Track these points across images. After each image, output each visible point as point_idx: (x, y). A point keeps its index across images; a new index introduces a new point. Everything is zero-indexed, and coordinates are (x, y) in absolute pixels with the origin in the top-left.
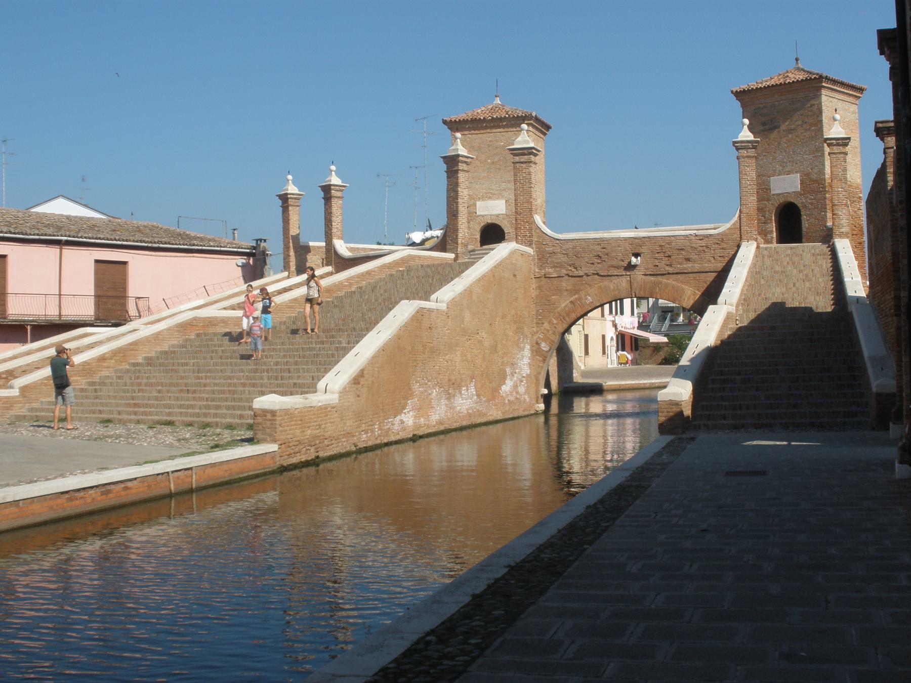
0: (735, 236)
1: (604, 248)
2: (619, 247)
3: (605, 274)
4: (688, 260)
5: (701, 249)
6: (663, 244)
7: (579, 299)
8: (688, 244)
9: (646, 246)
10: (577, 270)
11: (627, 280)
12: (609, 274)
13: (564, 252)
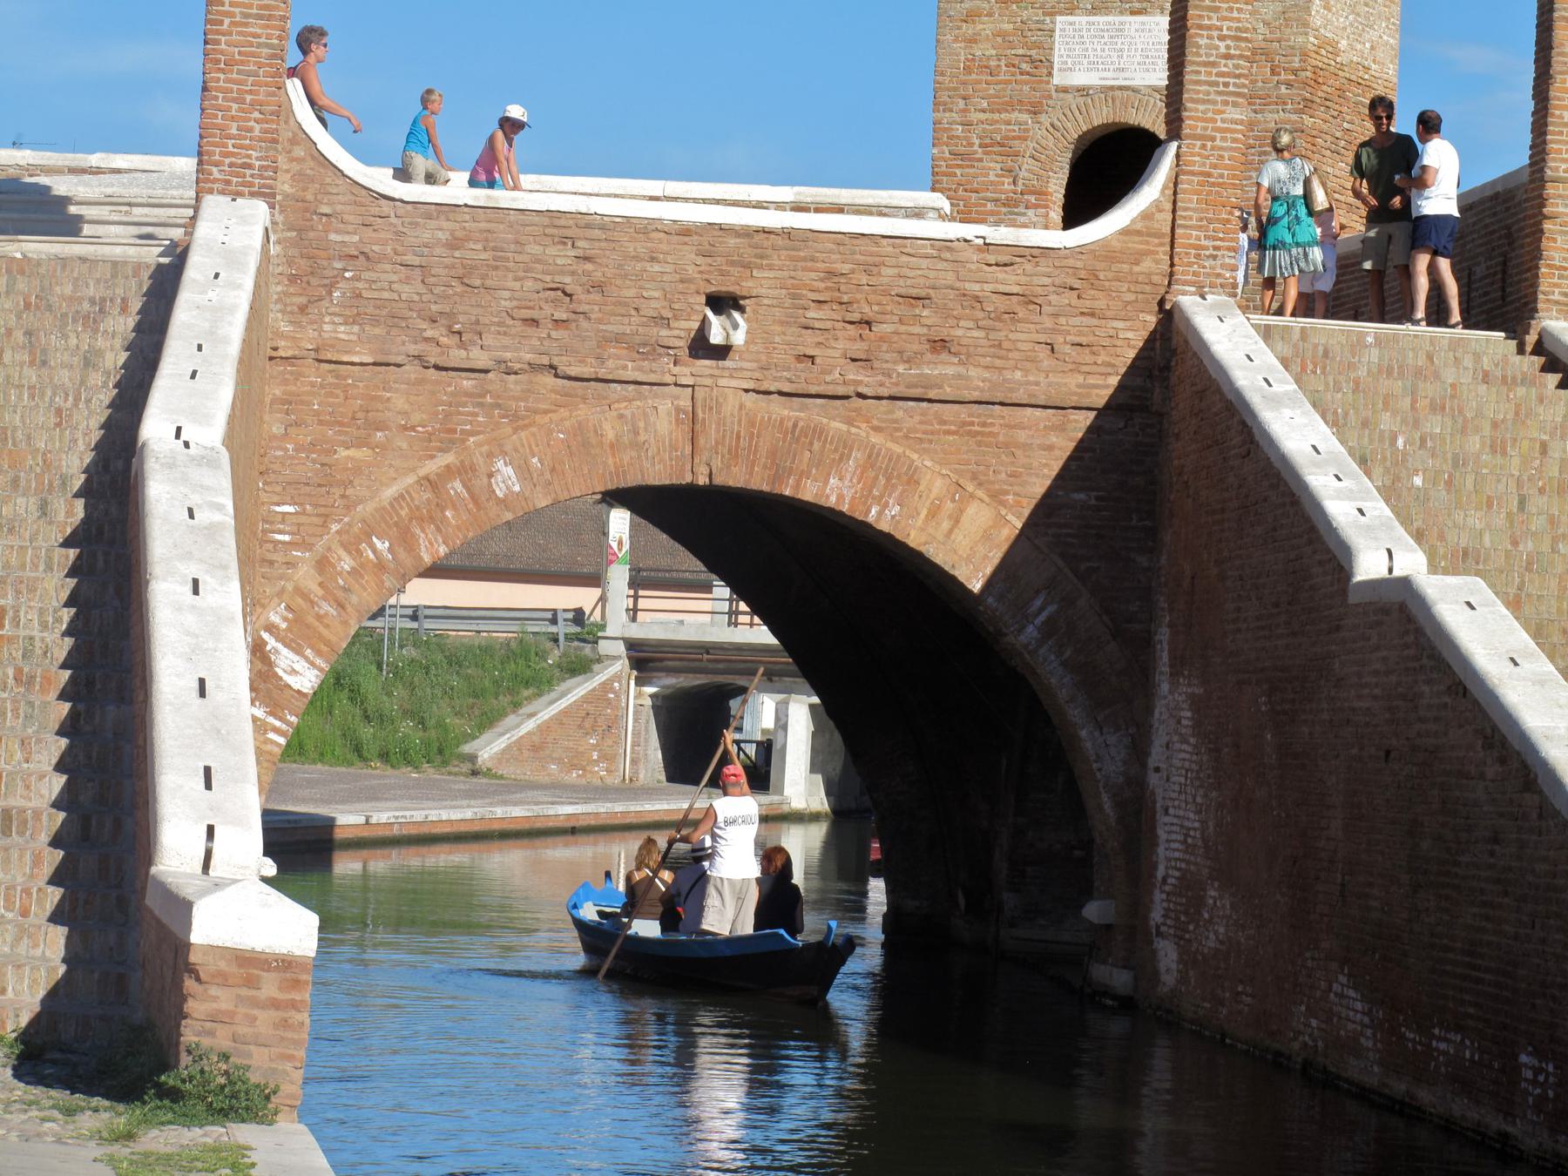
0: (1147, 265)
1: (587, 259)
2: (653, 259)
3: (585, 371)
4: (940, 345)
5: (1002, 304)
6: (845, 268)
7: (464, 471)
8: (950, 278)
9: (771, 268)
10: (462, 345)
11: (678, 410)
12: (602, 373)
13: (410, 259)
